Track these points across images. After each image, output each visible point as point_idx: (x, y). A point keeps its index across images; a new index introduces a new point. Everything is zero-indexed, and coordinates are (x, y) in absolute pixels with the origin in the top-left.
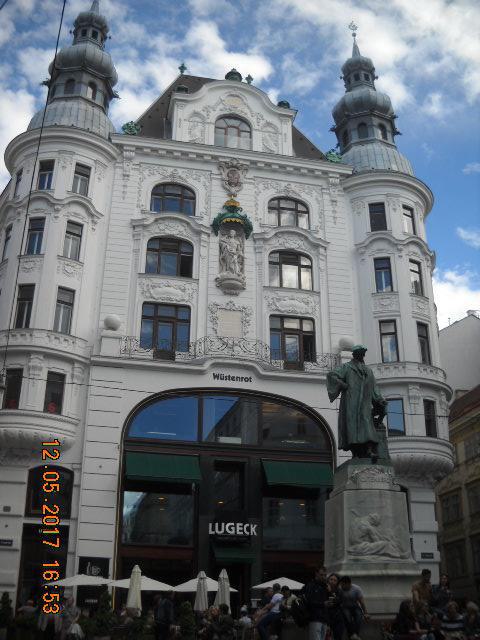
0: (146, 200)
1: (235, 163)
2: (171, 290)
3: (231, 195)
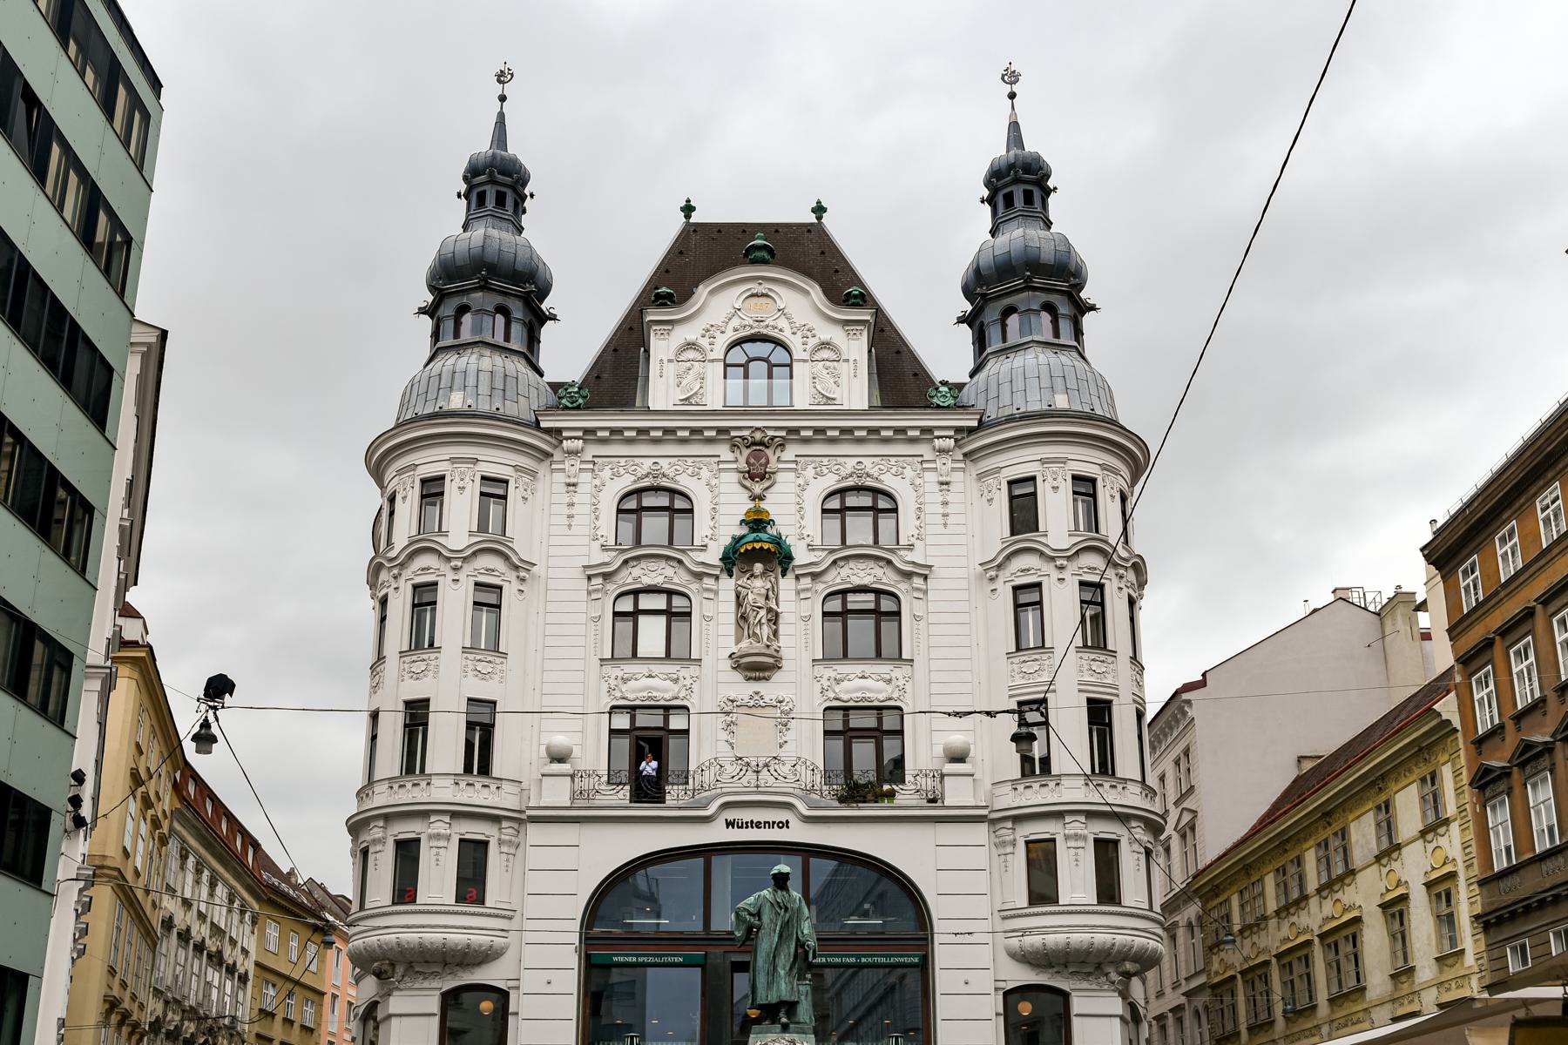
1: (758, 436)
3: (754, 498)
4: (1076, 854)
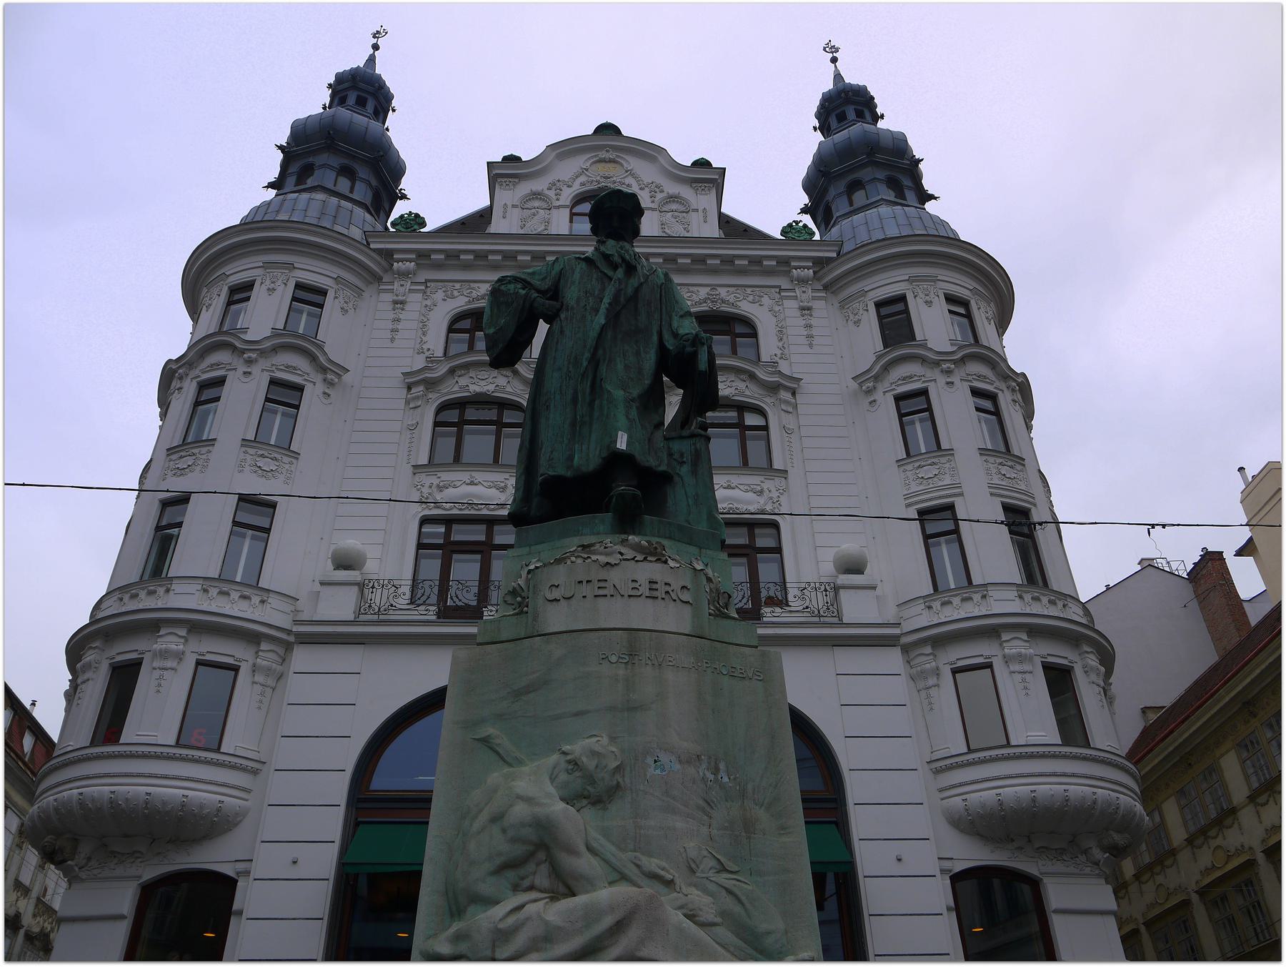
4: (1024, 681)
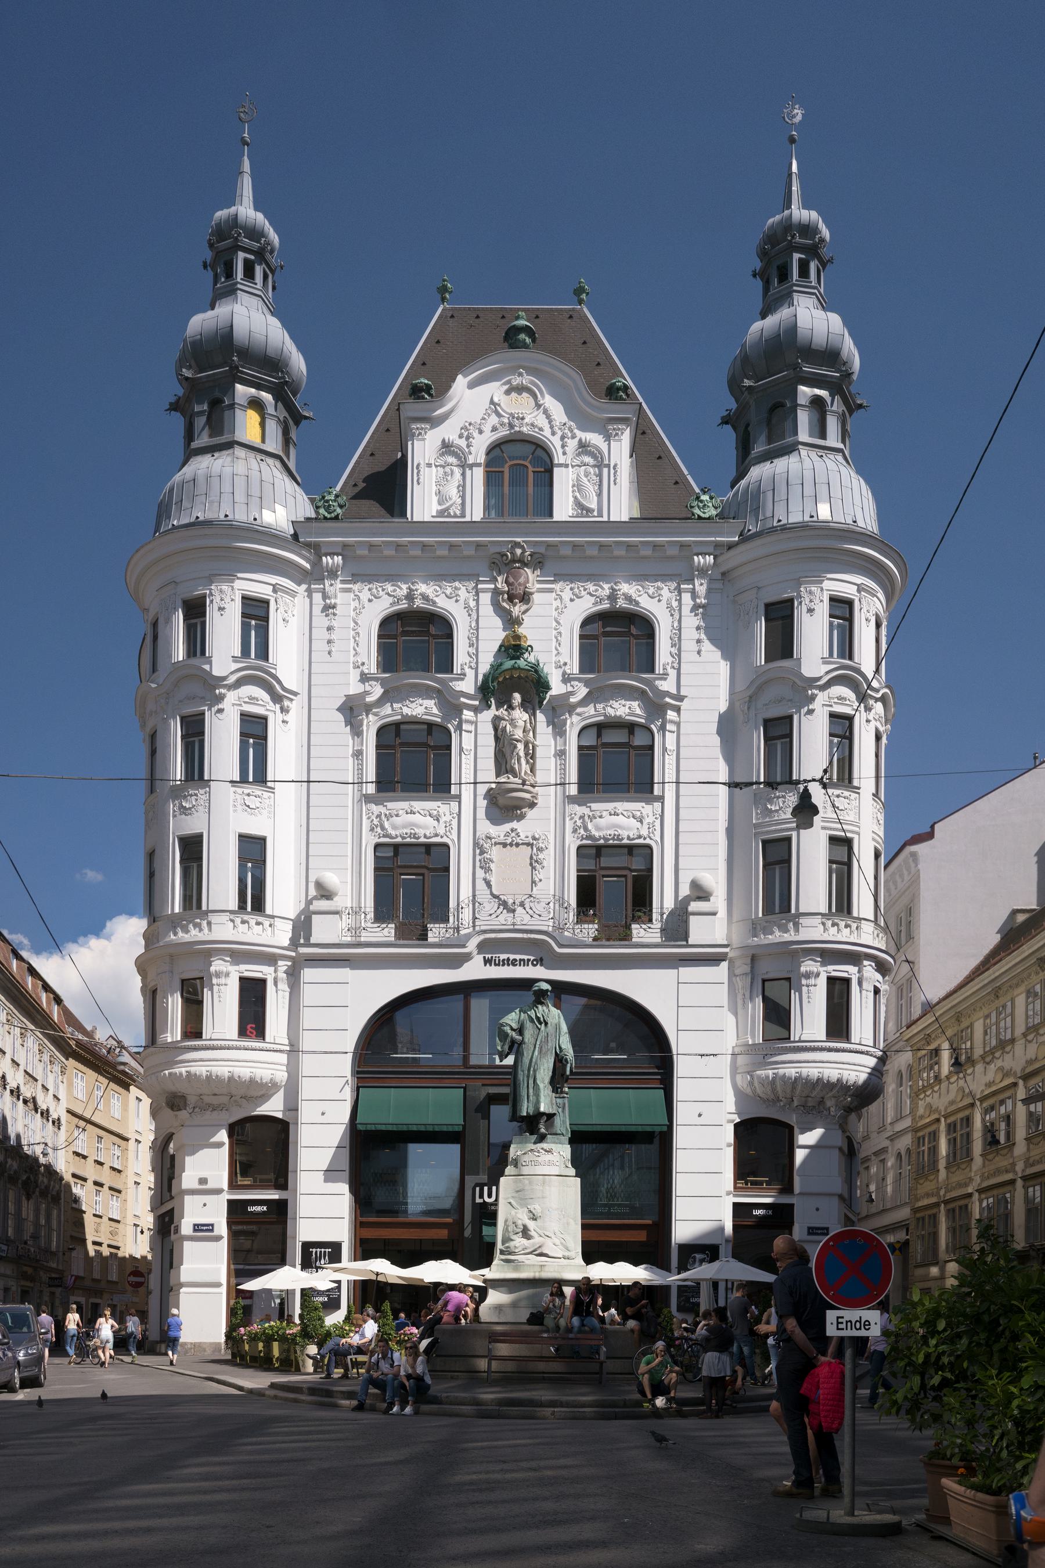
0: (370, 658)
2: (416, 818)
